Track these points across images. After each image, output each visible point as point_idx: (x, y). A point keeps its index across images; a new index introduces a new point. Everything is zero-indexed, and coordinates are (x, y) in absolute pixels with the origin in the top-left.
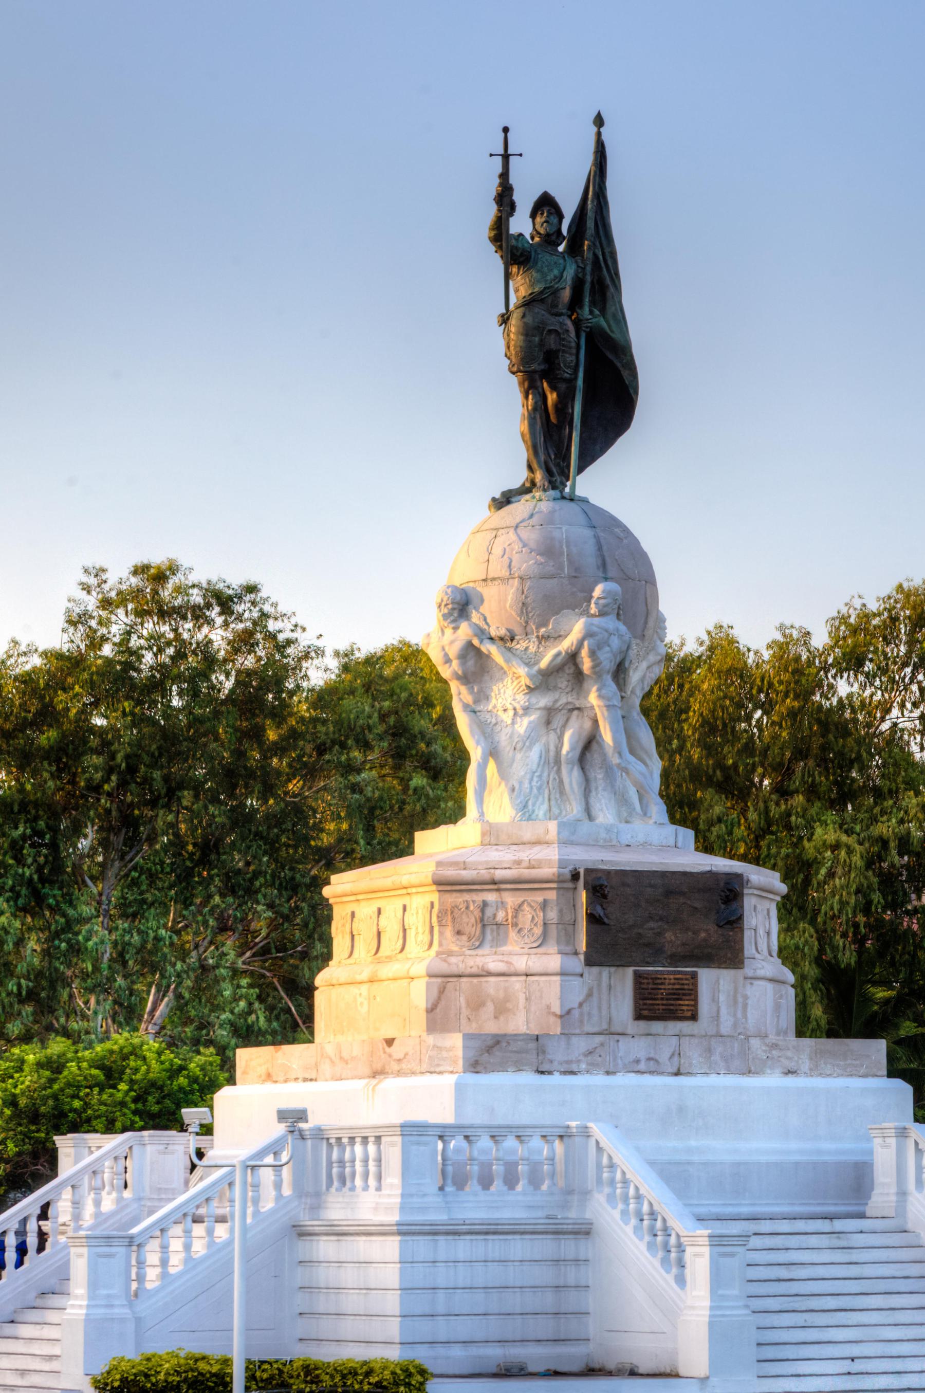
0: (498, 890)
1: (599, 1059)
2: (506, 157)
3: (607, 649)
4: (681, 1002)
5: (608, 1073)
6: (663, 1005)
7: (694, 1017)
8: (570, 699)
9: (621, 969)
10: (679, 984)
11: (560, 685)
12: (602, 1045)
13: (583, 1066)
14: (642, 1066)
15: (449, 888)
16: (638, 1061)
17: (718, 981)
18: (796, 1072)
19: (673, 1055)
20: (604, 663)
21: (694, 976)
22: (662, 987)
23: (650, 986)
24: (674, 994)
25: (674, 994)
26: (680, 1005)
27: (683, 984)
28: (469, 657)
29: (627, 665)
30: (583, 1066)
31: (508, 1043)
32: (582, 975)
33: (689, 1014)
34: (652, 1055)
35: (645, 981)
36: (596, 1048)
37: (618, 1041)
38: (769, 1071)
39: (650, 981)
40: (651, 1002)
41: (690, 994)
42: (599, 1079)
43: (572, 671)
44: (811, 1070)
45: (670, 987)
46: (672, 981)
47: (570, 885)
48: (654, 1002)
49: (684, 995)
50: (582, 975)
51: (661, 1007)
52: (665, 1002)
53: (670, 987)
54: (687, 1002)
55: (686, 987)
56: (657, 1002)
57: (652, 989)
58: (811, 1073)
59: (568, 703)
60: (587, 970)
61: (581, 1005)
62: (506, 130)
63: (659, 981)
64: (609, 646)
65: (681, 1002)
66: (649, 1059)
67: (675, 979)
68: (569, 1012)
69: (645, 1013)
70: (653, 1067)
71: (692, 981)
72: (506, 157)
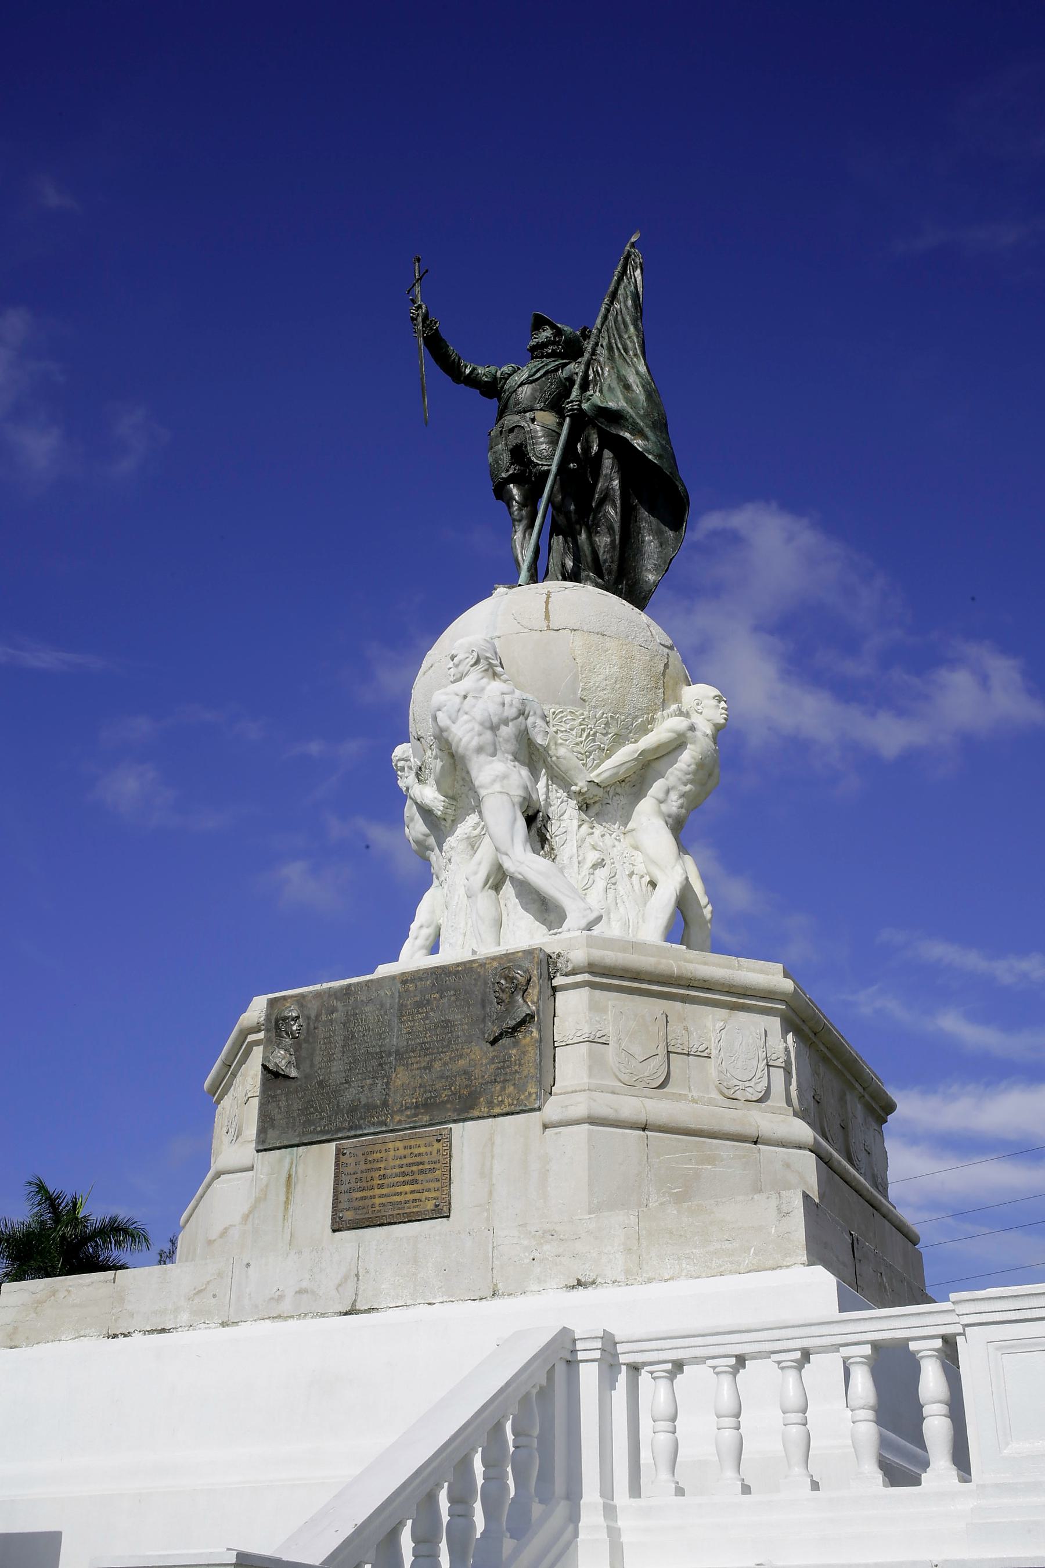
1: (213, 1301)
3: (466, 717)
5: (224, 1324)
6: (381, 1196)
7: (441, 1212)
12: (220, 1275)
13: (184, 1317)
14: (286, 1307)
16: (280, 1298)
17: (491, 1141)
18: (593, 1283)
19: (346, 1278)
20: (465, 740)
21: (444, 1140)
22: (382, 1165)
24: (404, 1174)
25: (404, 1174)
29: (539, 740)
30: (184, 1317)
31: (69, 1291)
33: (430, 1205)
34: (304, 1284)
36: (208, 1282)
37: (248, 1265)
38: (535, 1287)
41: (433, 1170)
42: (209, 1337)
44: (627, 1272)
45: (398, 1162)
46: (402, 1152)
49: (422, 1172)
53: (398, 1162)
58: (630, 1278)
61: (246, 1218)
63: (378, 1156)
66: (300, 1292)
68: (226, 1231)
69: (348, 1215)
70: (305, 1305)
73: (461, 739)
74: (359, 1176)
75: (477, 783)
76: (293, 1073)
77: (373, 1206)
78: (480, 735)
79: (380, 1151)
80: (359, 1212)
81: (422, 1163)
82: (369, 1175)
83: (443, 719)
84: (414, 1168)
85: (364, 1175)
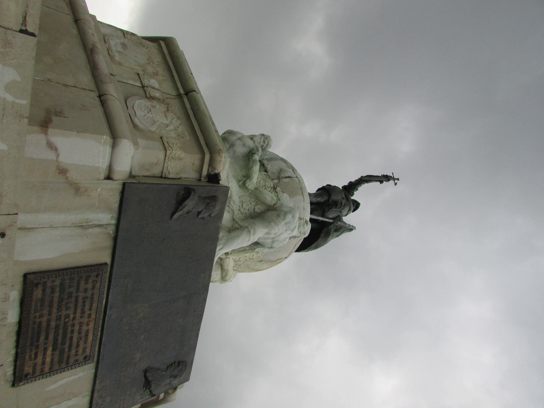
0: (179, 96)
2: (394, 179)
4: (49, 352)
8: (236, 212)
9: (109, 243)
10: (79, 338)
11: (245, 204)
15: (166, 52)
21: (86, 359)
23: (81, 295)
26: (45, 350)
27: (78, 346)
28: (244, 148)
29: (257, 250)
32: (109, 178)
35: (90, 286)
39: (89, 294)
40: (56, 300)
43: (257, 210)
45: (77, 328)
47: (205, 172)
48: (55, 305)
50: (109, 178)
51: (45, 319)
52: (53, 324)
54: (48, 360)
55: (73, 352)
56: (55, 310)
57: (77, 297)
59: (233, 210)
60: (115, 187)
62: (398, 179)
64: (286, 230)
65: (49, 352)
67: (88, 331)
69: (38, 293)
71: (81, 358)
72: (394, 179)
73: (277, 226)
74: (74, 295)
75: (256, 228)
76: (176, 216)
77: (41, 316)
78: (275, 234)
79: (90, 309)
80: (39, 304)
81: (70, 350)
82: (72, 305)
83: (289, 217)
84: (67, 345)
85: (73, 299)
